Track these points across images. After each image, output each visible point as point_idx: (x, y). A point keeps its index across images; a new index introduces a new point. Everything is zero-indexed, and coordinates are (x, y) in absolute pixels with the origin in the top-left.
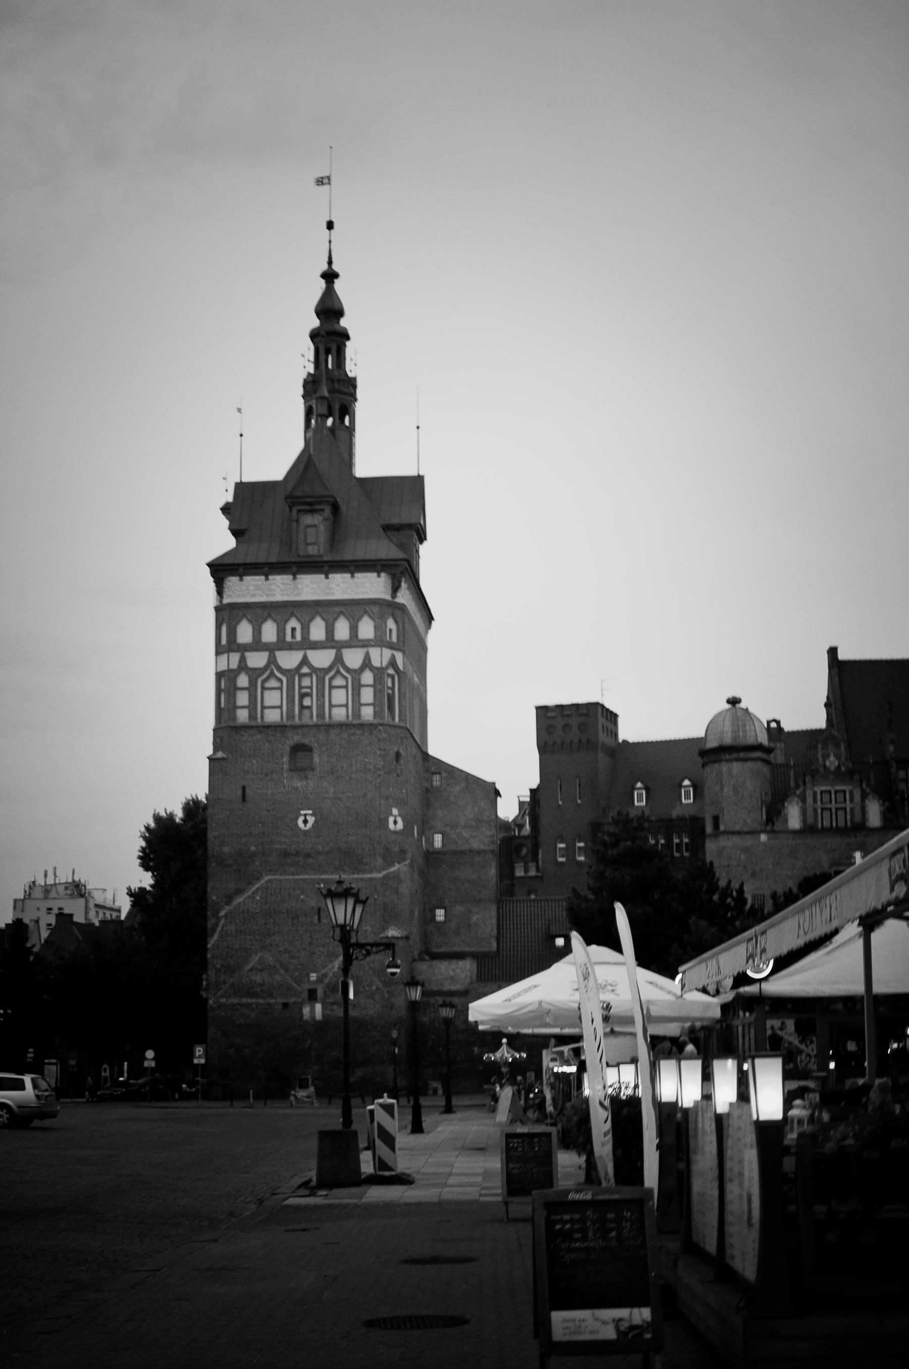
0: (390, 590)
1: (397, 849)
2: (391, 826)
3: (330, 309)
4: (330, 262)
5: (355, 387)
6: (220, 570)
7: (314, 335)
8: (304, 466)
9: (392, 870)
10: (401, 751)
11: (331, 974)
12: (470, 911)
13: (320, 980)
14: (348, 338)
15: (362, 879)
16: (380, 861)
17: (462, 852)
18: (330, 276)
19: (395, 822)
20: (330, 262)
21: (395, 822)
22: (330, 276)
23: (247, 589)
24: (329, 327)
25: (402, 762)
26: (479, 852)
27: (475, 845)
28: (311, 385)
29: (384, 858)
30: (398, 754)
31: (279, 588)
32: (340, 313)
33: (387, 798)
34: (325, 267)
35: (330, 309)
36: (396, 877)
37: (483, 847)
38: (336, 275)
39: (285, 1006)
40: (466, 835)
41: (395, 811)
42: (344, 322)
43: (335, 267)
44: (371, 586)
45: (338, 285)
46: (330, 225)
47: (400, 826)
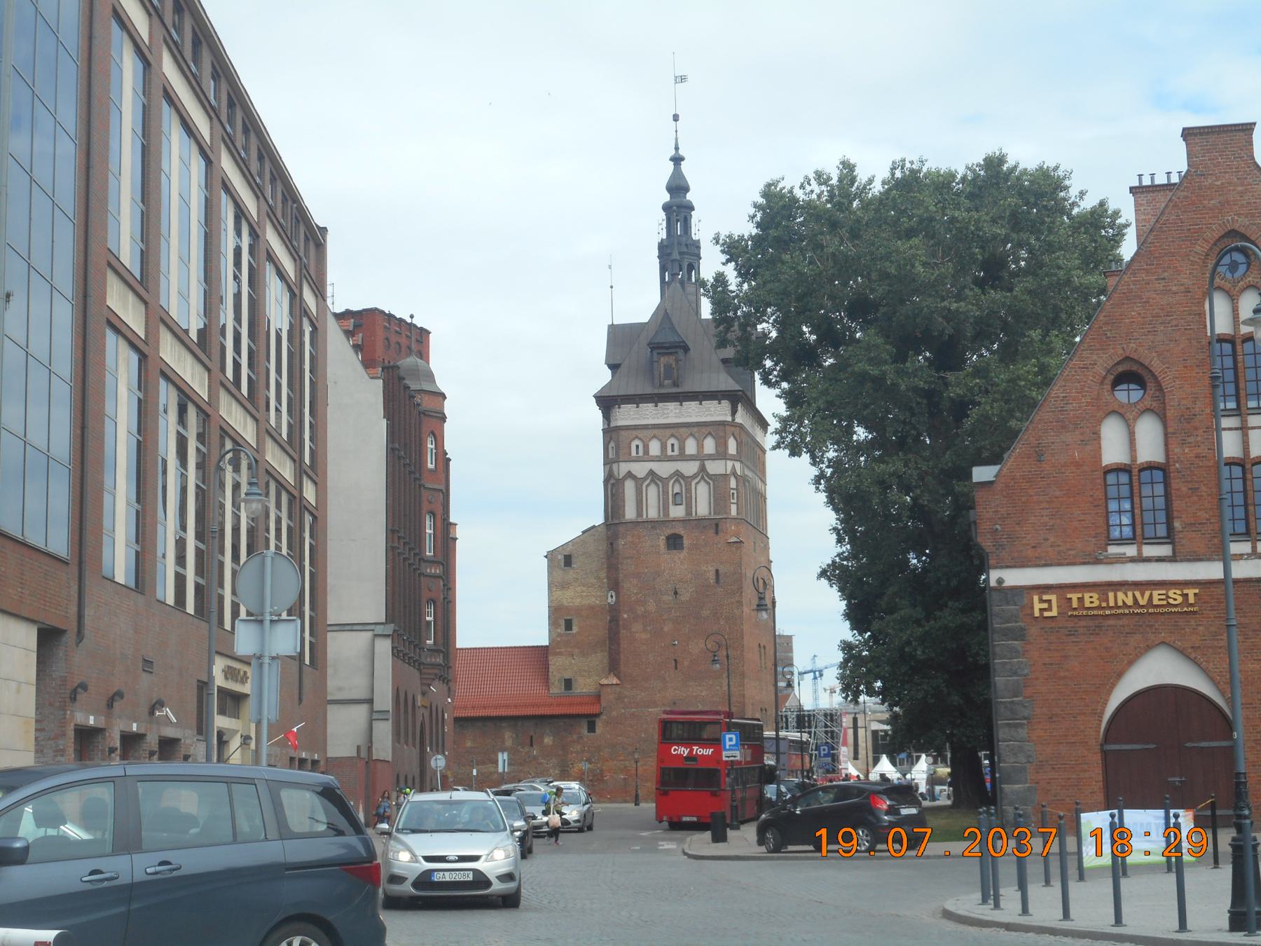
3: (678, 187)
4: (677, 148)
5: (699, 248)
6: (607, 402)
7: (666, 208)
8: (663, 315)
14: (692, 208)
18: (677, 160)
20: (677, 148)
22: (677, 160)
23: (626, 415)
24: (677, 200)
28: (665, 250)
31: (648, 414)
32: (687, 189)
34: (673, 152)
35: (678, 187)
38: (683, 159)
42: (689, 196)
43: (681, 152)
44: (717, 411)
45: (684, 166)
46: (676, 118)
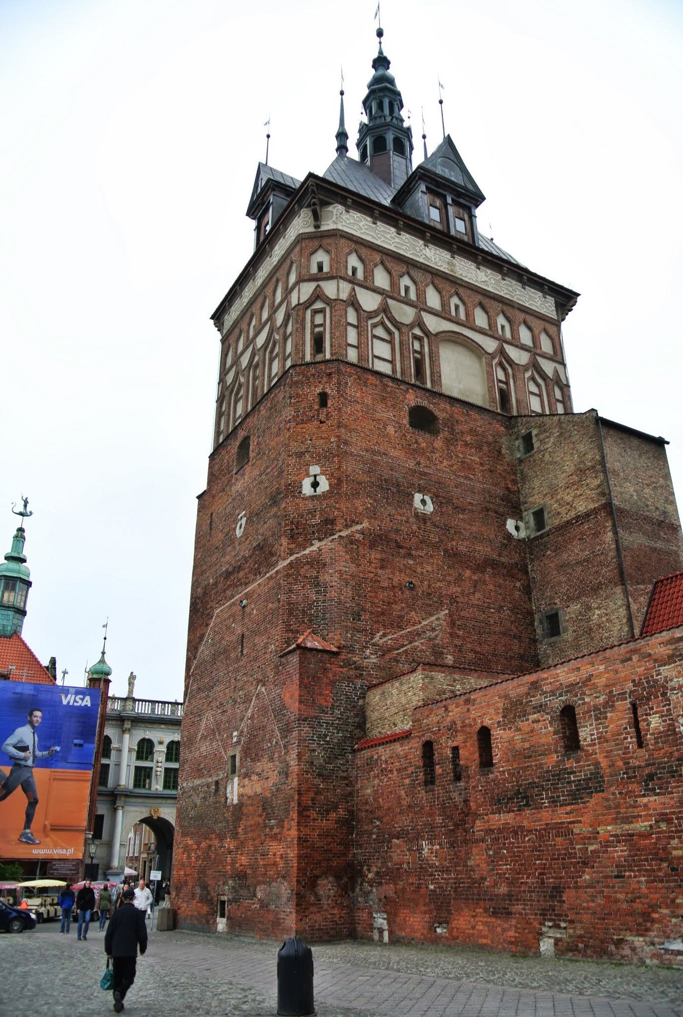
0: (311, 221)
1: (317, 520)
2: (307, 490)
9: (307, 552)
10: (328, 391)
11: (245, 730)
12: (589, 608)
13: (238, 742)
15: (271, 578)
16: (284, 541)
17: (568, 522)
19: (315, 485)
21: (315, 485)
25: (330, 403)
26: (587, 515)
27: (582, 507)
29: (292, 537)
30: (323, 398)
33: (300, 455)
36: (317, 562)
37: (592, 506)
39: (217, 783)
40: (569, 499)
41: (315, 469)
47: (324, 485)
